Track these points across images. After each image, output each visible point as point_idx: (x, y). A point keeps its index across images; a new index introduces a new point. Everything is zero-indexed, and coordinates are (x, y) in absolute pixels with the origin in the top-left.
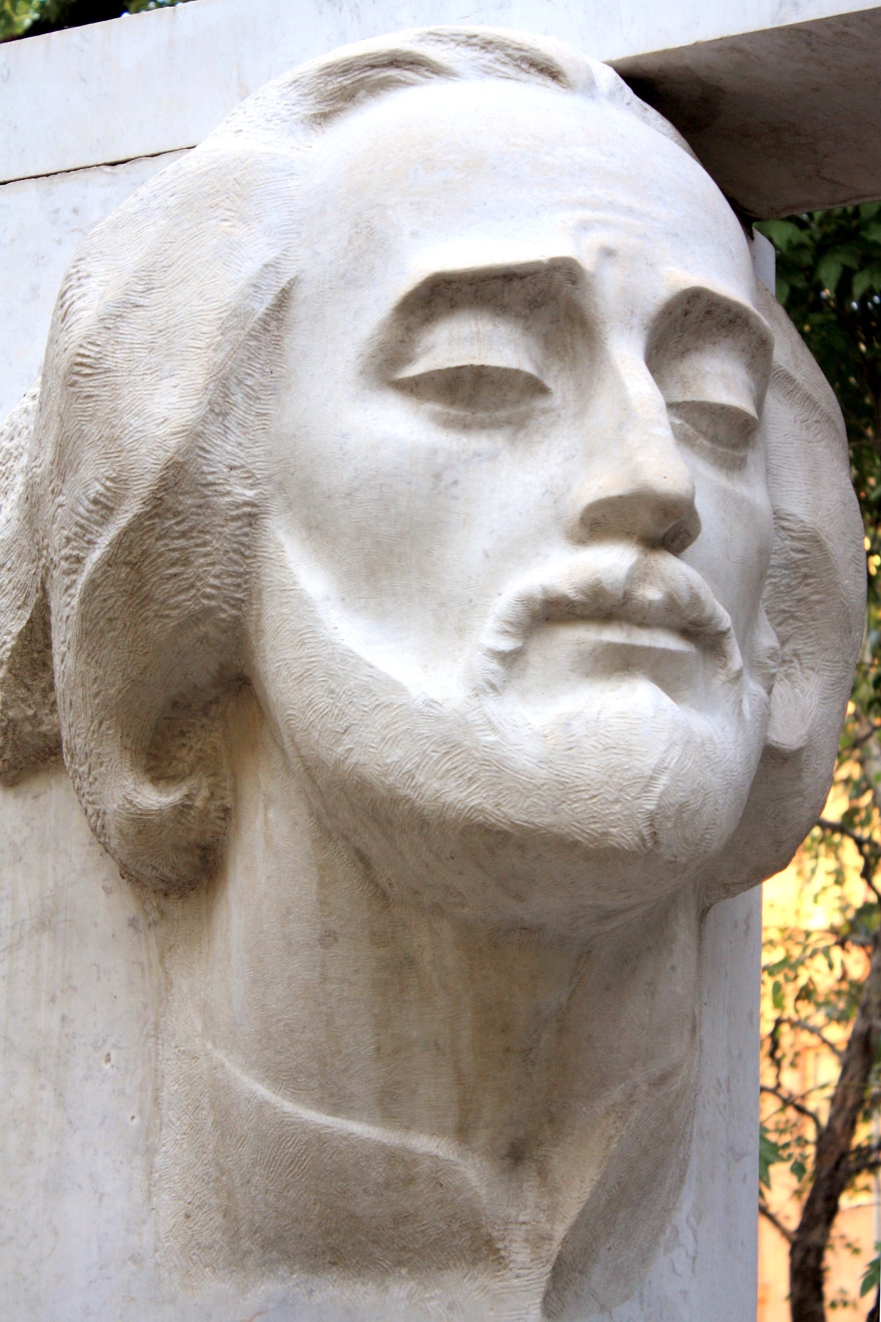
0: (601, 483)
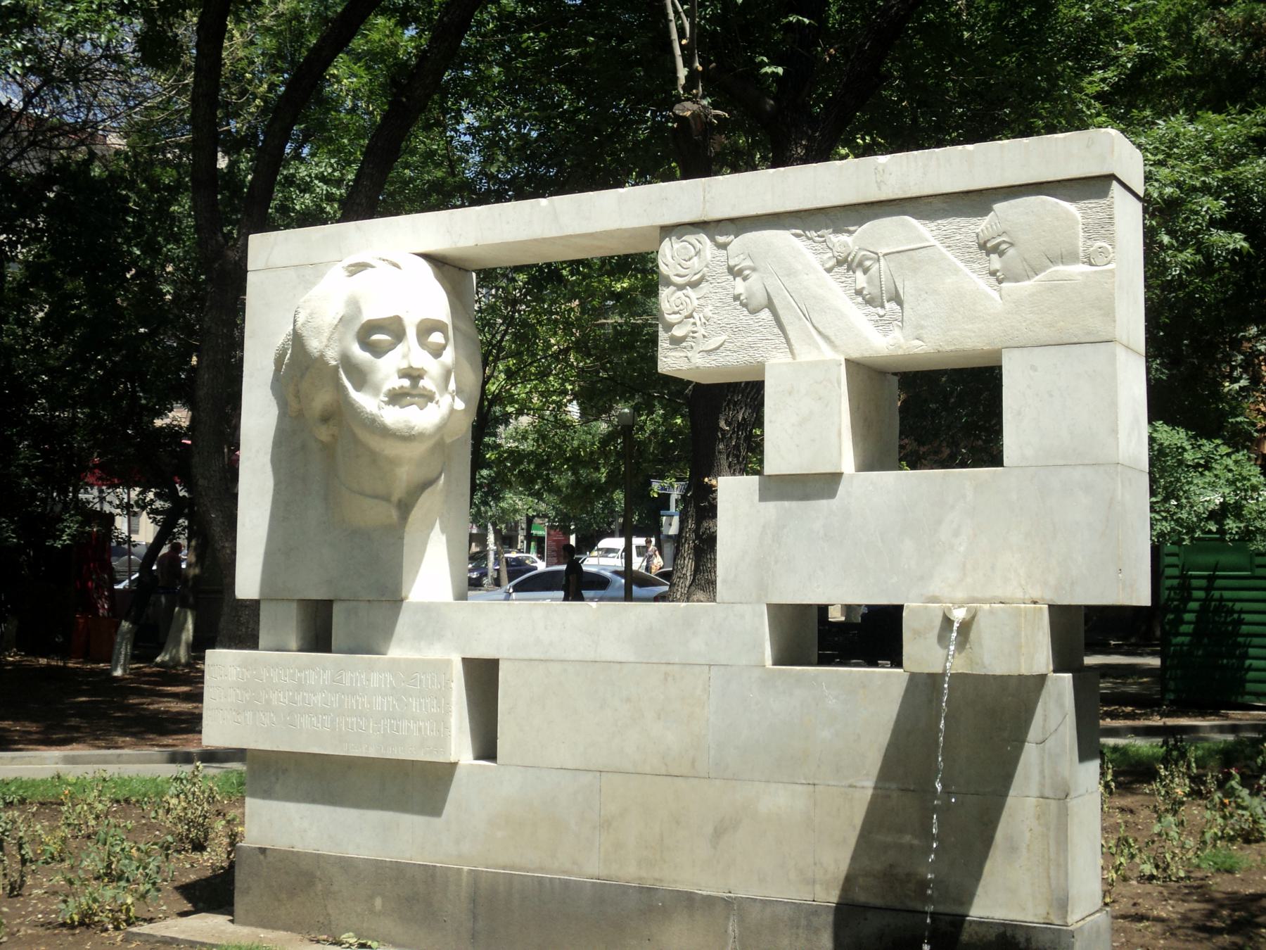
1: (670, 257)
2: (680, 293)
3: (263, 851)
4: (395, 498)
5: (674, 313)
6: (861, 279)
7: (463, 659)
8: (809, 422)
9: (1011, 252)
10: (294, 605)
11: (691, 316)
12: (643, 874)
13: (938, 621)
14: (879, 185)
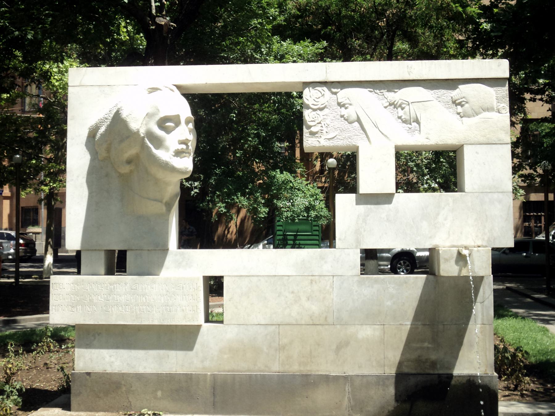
1: (309, 96)
2: (314, 113)
3: (89, 374)
4: (164, 201)
5: (312, 121)
6: (401, 112)
8: (376, 172)
11: (320, 123)
12: (302, 369)
13: (455, 255)
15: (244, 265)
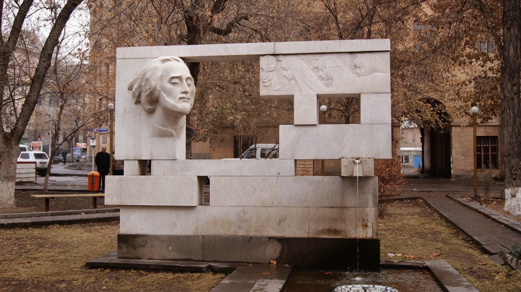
0: (183, 90)
2: (267, 74)
7: (198, 176)
8: (306, 110)
9: (363, 69)
10: (137, 161)
14: (327, 48)
15: (222, 168)
